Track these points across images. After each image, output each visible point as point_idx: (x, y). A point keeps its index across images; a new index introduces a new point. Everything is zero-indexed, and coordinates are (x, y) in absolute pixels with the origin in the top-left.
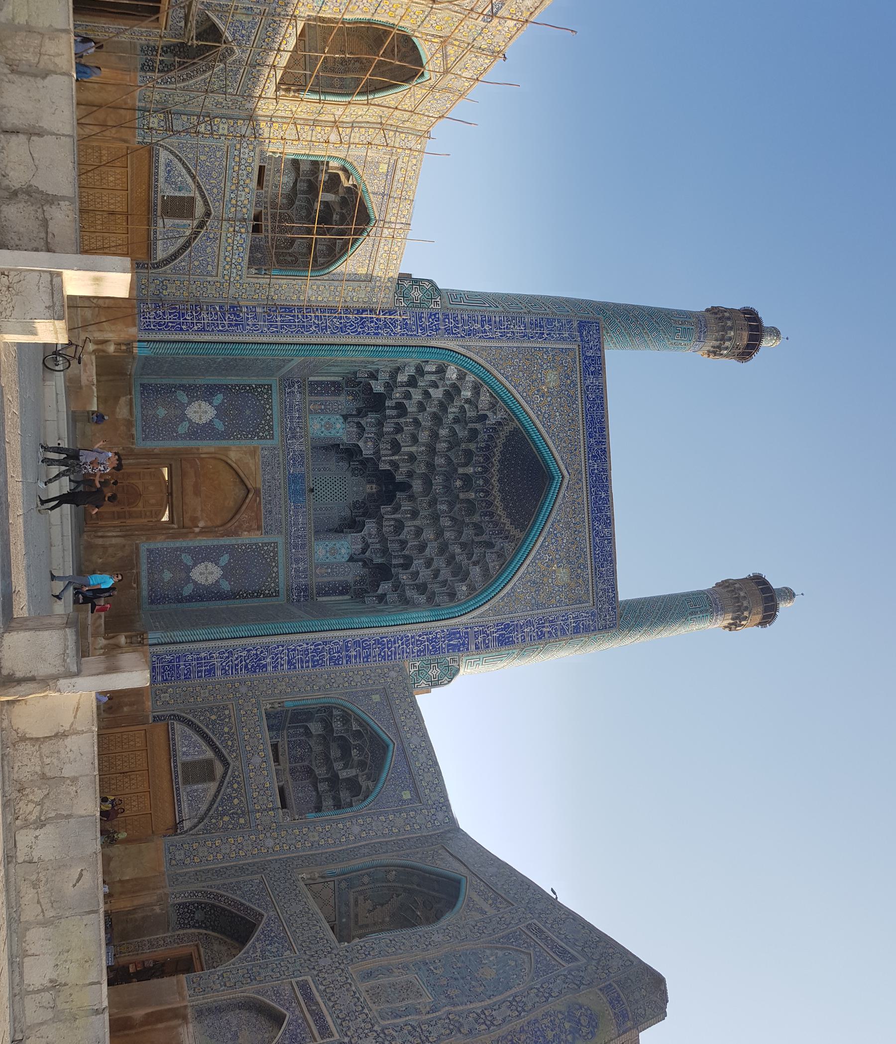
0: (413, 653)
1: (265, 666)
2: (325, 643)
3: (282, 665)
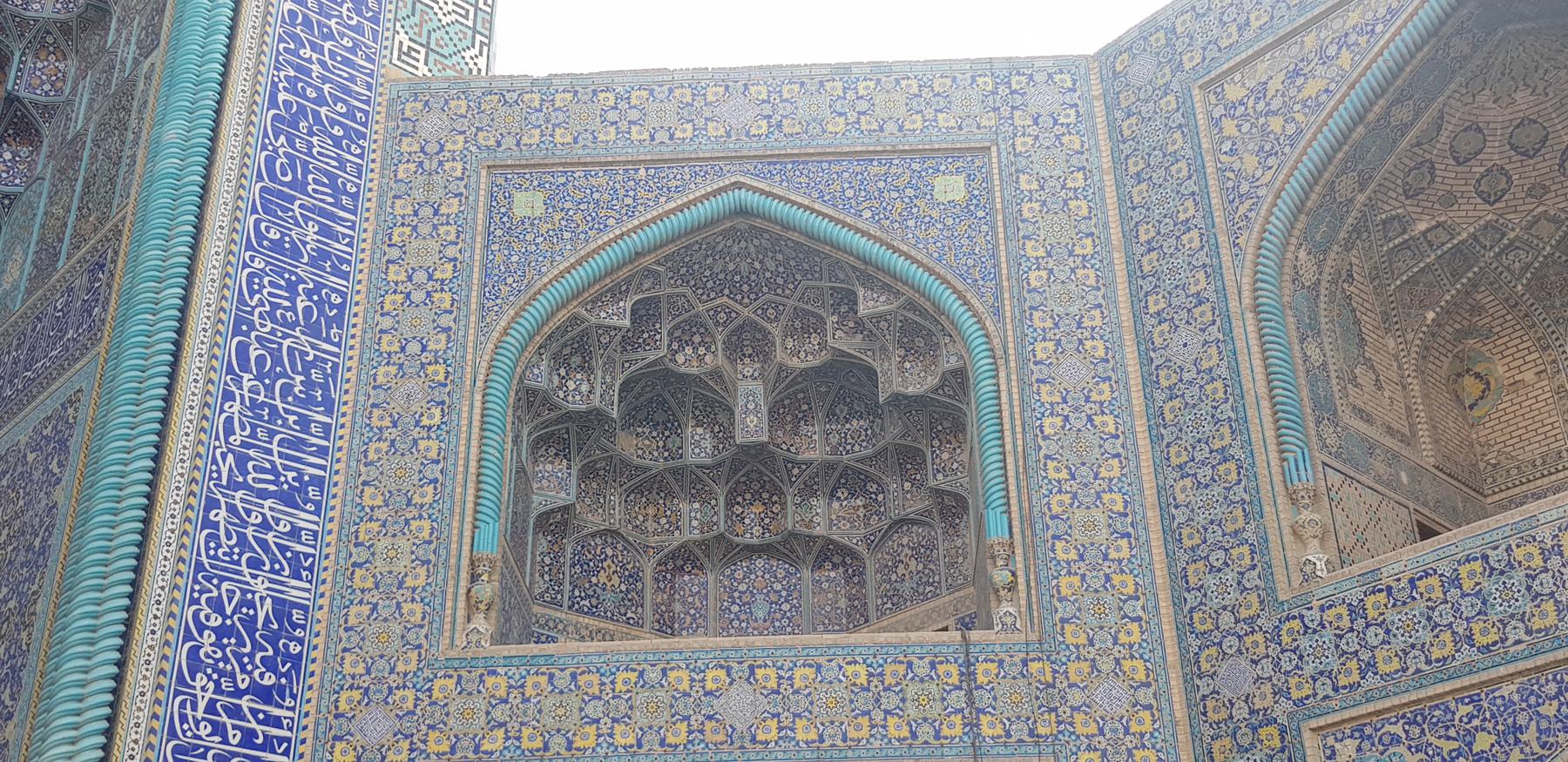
0: (358, 29)
1: (282, 608)
2: (241, 325)
3: (295, 533)
